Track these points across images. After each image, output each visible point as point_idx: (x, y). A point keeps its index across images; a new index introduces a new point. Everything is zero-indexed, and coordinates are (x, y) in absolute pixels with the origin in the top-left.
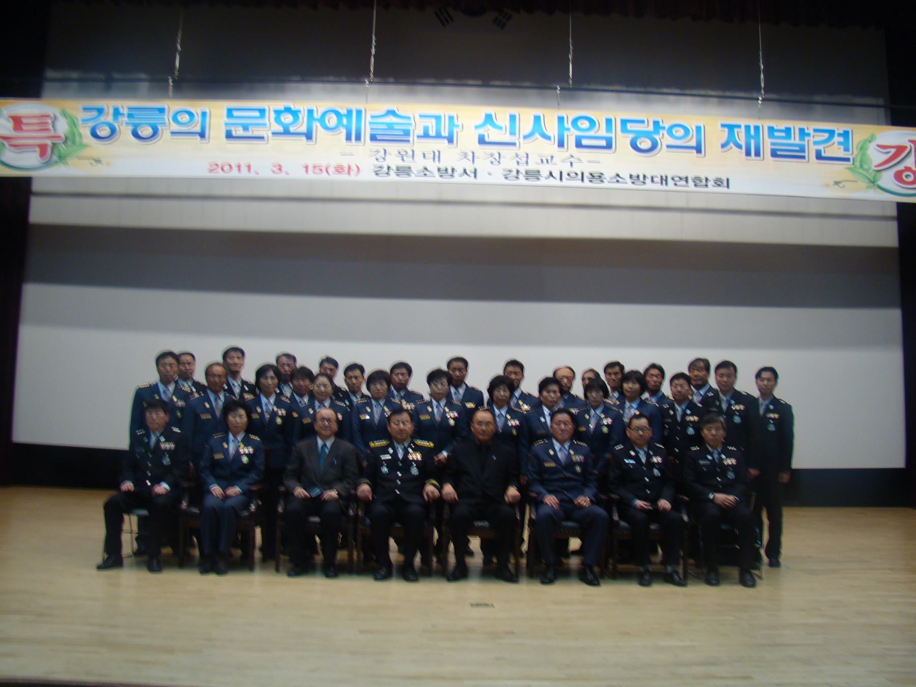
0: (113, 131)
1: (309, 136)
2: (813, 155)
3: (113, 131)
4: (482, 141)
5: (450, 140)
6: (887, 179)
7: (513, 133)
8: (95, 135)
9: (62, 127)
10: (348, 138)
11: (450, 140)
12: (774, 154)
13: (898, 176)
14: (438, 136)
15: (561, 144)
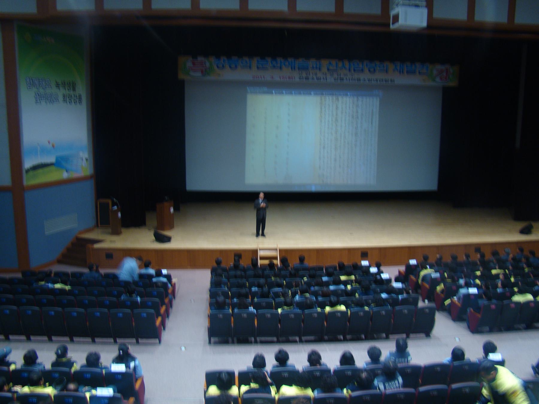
0: (223, 66)
1: (281, 68)
2: (418, 73)
3: (223, 66)
4: (328, 69)
5: (320, 69)
6: (438, 79)
7: (336, 67)
8: (218, 67)
9: (208, 64)
10: (292, 68)
11: (320, 69)
12: (408, 72)
13: (441, 79)
14: (316, 68)
15: (350, 70)
